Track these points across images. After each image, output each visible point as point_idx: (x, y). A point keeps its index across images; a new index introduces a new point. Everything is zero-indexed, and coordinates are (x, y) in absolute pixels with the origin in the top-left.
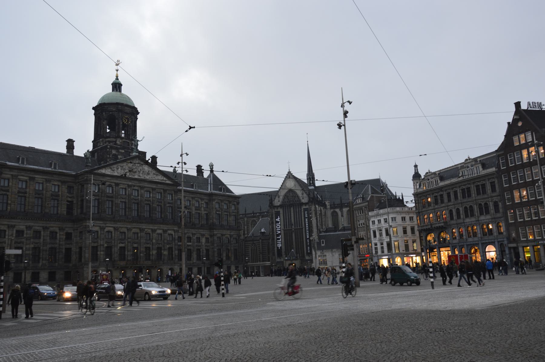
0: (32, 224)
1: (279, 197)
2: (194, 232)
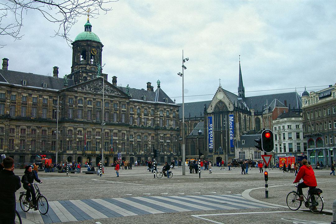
0: (31, 125)
1: (211, 106)
2: (143, 132)
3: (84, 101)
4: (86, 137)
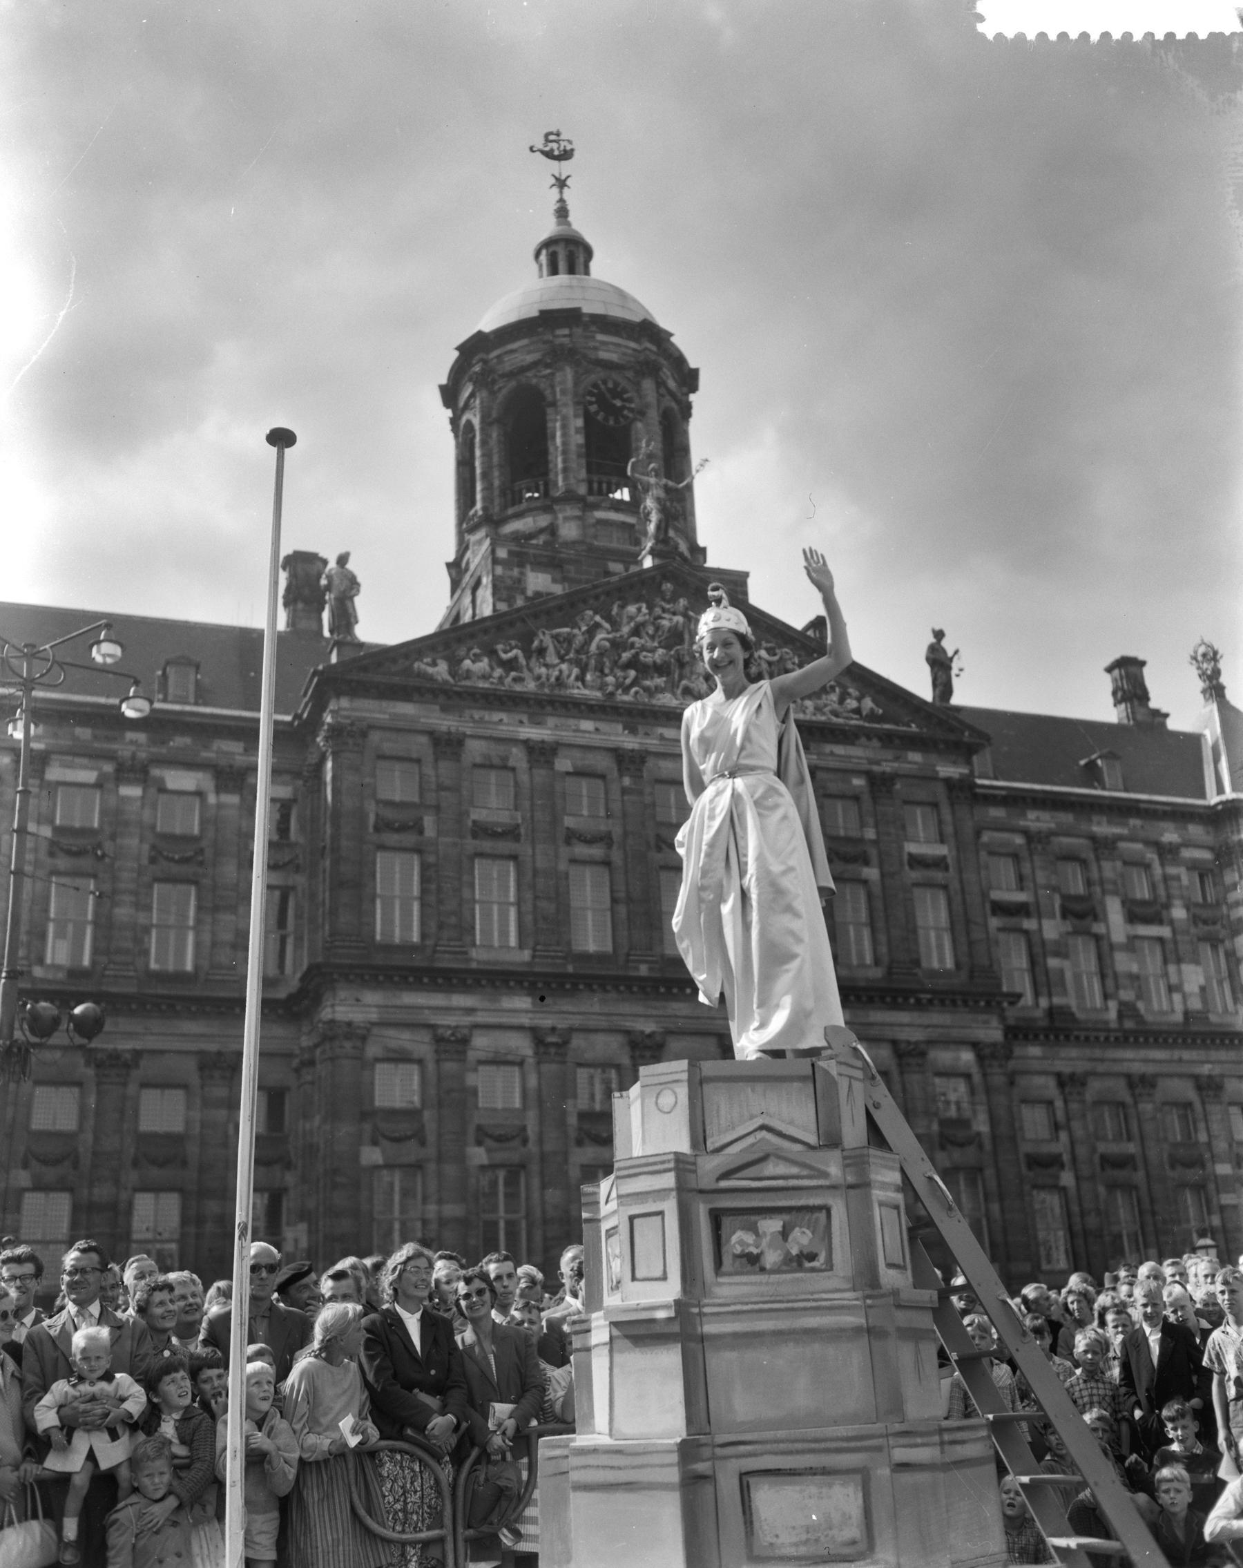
2: (1137, 1068)
3: (524, 778)
4: (573, 1120)
